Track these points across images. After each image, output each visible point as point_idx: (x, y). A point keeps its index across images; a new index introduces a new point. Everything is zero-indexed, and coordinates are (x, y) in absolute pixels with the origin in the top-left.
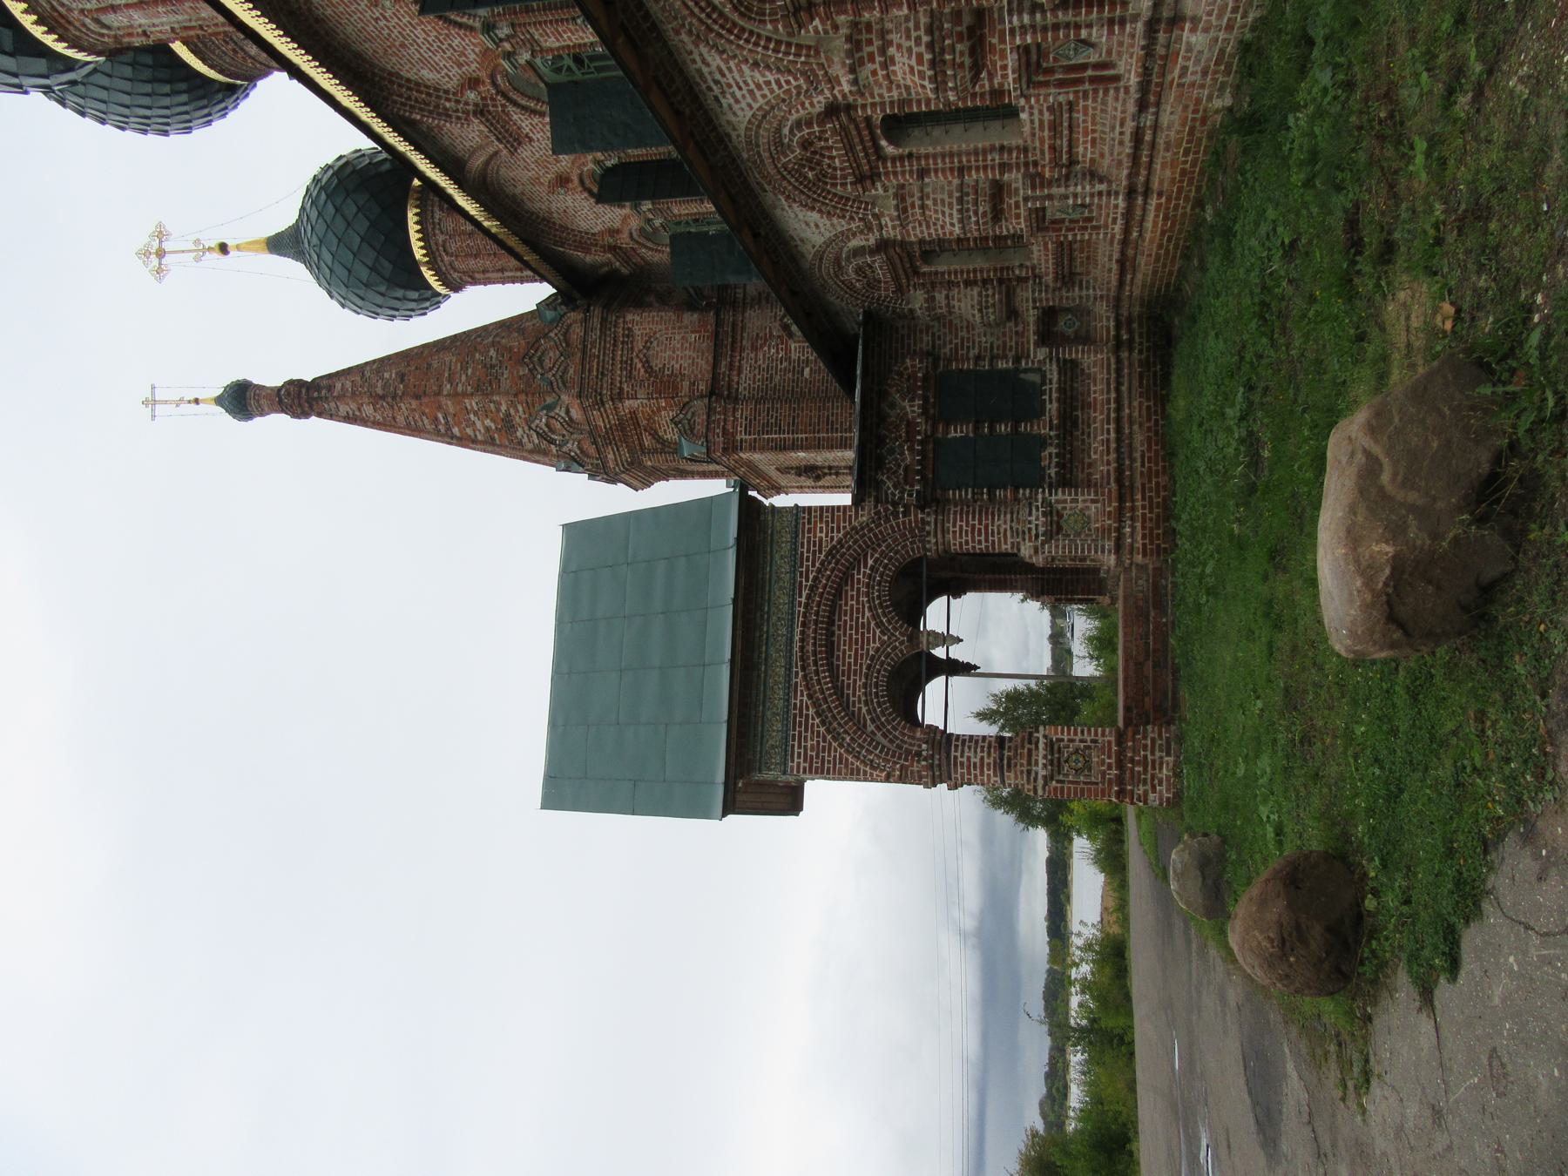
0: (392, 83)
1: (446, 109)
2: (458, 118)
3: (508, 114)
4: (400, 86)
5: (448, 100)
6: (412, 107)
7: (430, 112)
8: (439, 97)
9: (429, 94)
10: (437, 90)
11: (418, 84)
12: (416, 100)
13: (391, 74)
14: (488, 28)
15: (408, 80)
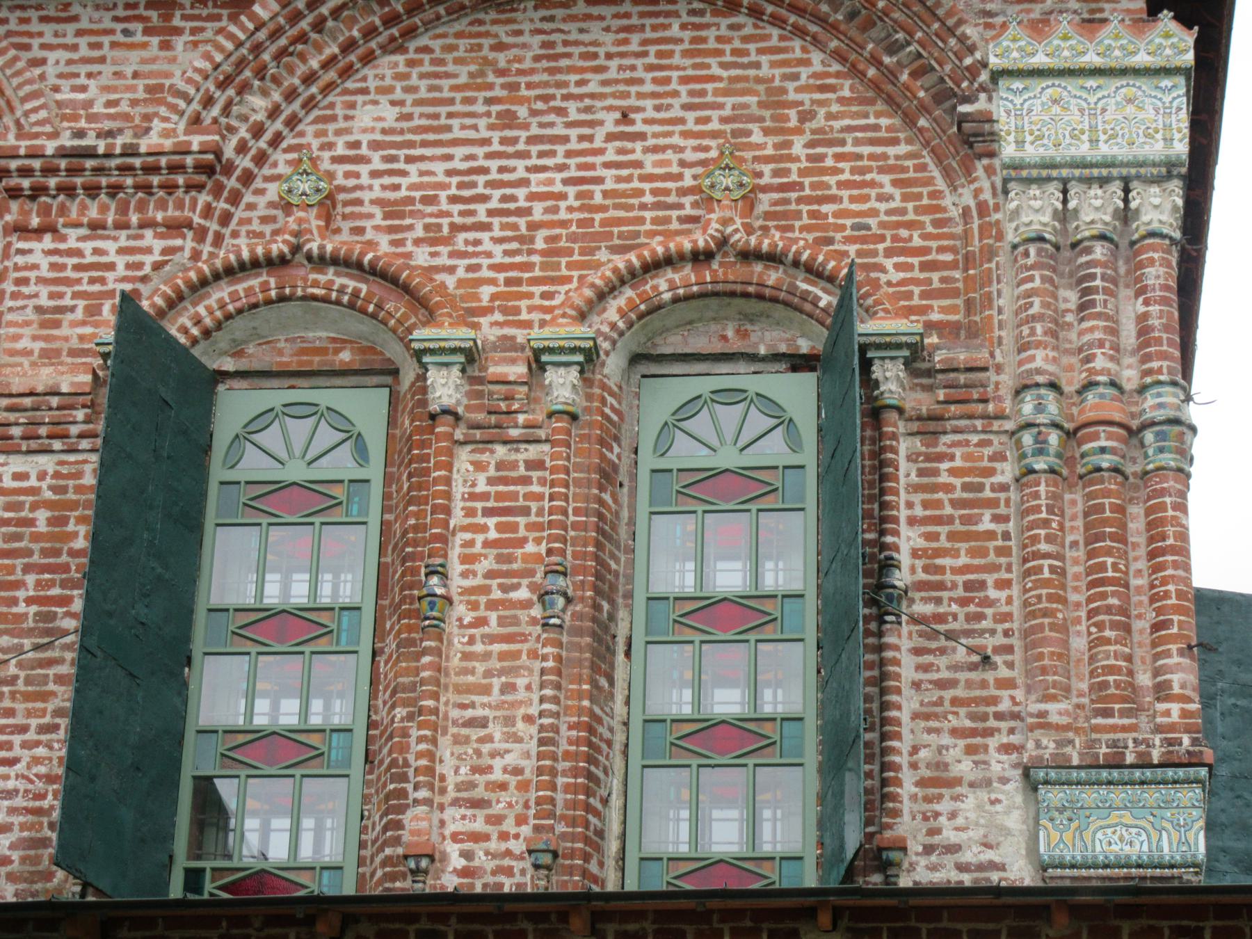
0: (390, 21)
1: (244, 88)
2: (208, 102)
3: (175, 227)
4: (370, 32)
5: (274, 113)
6: (296, 17)
7: (257, 49)
8: (290, 95)
9: (309, 79)
10: (309, 104)
11: (347, 72)
12: (302, 38)
13: (410, 33)
14: (590, 358)
15: (368, 59)
